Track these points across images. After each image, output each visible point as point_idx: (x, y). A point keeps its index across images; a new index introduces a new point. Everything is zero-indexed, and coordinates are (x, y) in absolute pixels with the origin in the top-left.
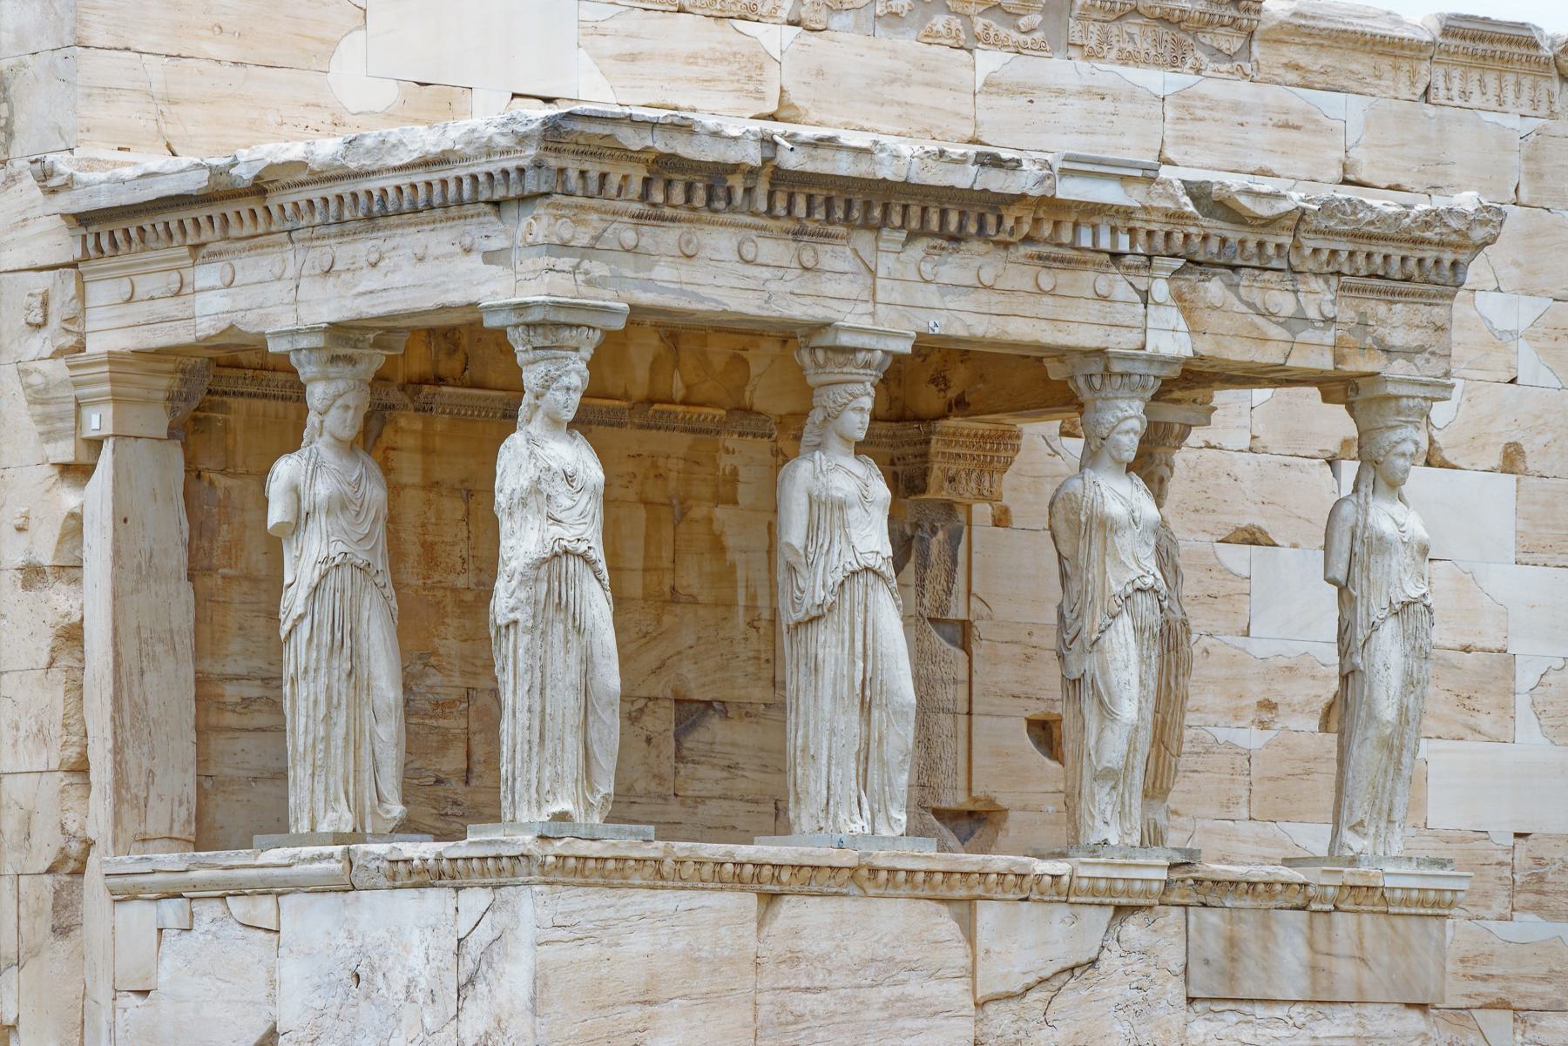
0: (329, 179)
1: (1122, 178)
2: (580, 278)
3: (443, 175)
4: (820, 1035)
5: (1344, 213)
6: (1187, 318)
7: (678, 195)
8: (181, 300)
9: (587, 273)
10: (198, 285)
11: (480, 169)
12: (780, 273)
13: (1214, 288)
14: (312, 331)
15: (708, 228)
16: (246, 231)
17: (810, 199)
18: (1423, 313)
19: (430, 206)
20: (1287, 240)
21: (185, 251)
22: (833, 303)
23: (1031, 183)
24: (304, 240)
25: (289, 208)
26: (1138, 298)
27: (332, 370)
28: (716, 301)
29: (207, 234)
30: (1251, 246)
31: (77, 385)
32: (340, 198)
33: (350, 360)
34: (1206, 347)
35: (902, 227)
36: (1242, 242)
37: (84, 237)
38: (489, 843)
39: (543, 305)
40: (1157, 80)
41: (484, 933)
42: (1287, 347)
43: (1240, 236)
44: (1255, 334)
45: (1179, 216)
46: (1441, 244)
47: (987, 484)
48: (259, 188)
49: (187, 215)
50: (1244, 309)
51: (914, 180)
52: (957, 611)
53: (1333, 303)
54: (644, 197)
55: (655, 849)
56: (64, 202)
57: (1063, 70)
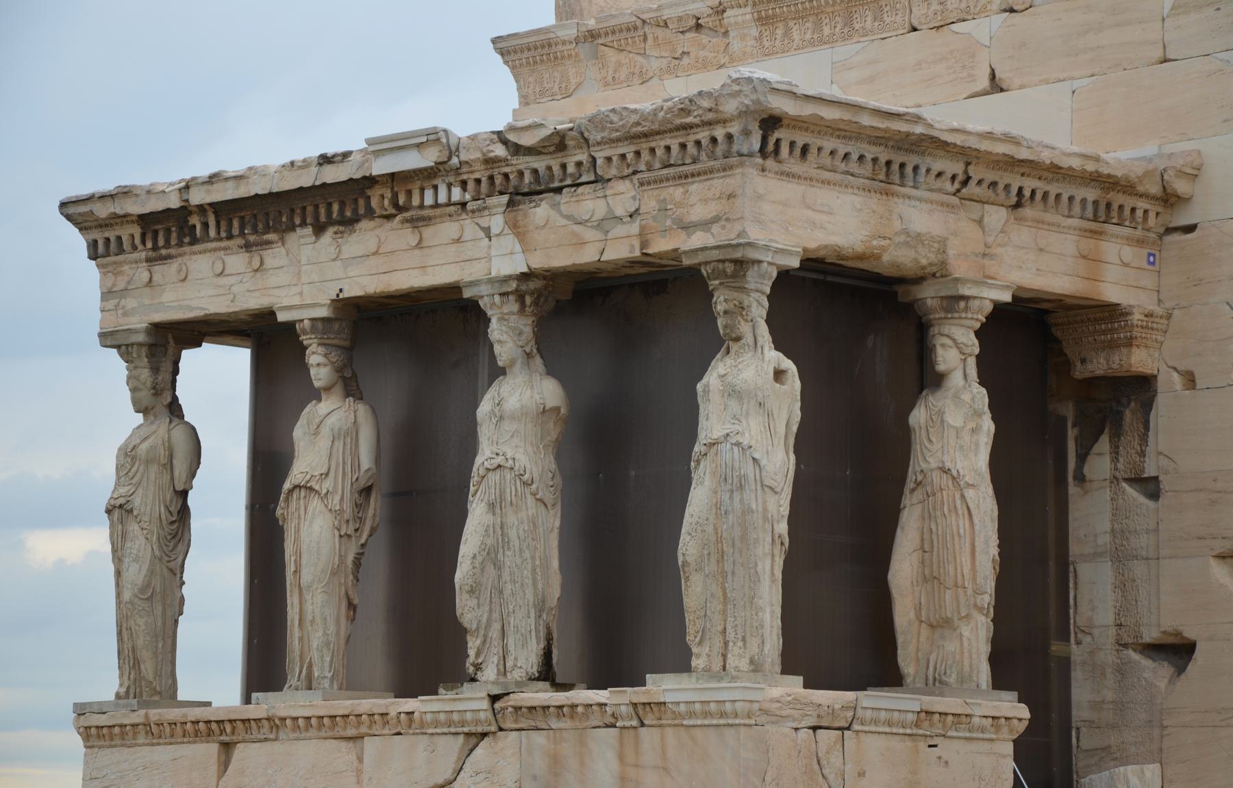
1: (418, 146)
5: (611, 123)
6: (521, 241)
9: (123, 307)
12: (239, 278)
13: (540, 212)
15: (194, 257)
17: (242, 218)
18: (718, 184)
20: (583, 157)
22: (276, 292)
23: (354, 168)
26: (482, 234)
28: (201, 309)
30: (556, 170)
35: (303, 224)
36: (549, 168)
42: (600, 245)
44: (574, 241)
45: (490, 162)
50: (565, 222)
52: (1150, 471)
53: (634, 198)
55: (138, 717)
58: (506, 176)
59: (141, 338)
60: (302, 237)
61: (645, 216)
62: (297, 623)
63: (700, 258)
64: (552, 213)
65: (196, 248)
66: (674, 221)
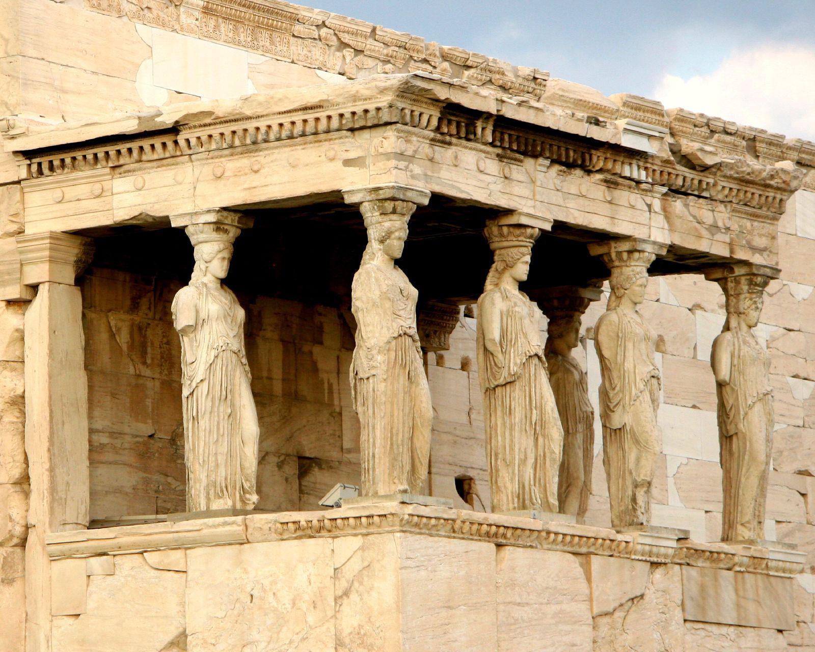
0: (226, 122)
1: (650, 136)
2: (408, 173)
3: (317, 115)
6: (668, 222)
7: (454, 130)
8: (103, 199)
10: (115, 191)
11: (347, 111)
13: (678, 205)
14: (209, 211)
16: (155, 157)
17: (510, 135)
20: (711, 181)
21: (108, 170)
22: (517, 199)
23: (610, 137)
24: (202, 159)
25: (193, 142)
26: (646, 208)
27: (215, 235)
30: (696, 182)
31: (21, 253)
32: (234, 132)
33: (226, 231)
34: (678, 241)
37: (29, 165)
38: (364, 507)
39: (393, 187)
41: (356, 565)
43: (692, 176)
44: (696, 234)
45: (667, 162)
46: (778, 189)
47: (443, 339)
48: (175, 130)
49: (112, 149)
50: (691, 218)
51: (562, 130)
54: (438, 129)
58: (669, 174)
60: (540, 165)
61: (732, 232)
62: (531, 461)
63: (762, 271)
64: (685, 210)
65: (470, 144)
66: (747, 241)
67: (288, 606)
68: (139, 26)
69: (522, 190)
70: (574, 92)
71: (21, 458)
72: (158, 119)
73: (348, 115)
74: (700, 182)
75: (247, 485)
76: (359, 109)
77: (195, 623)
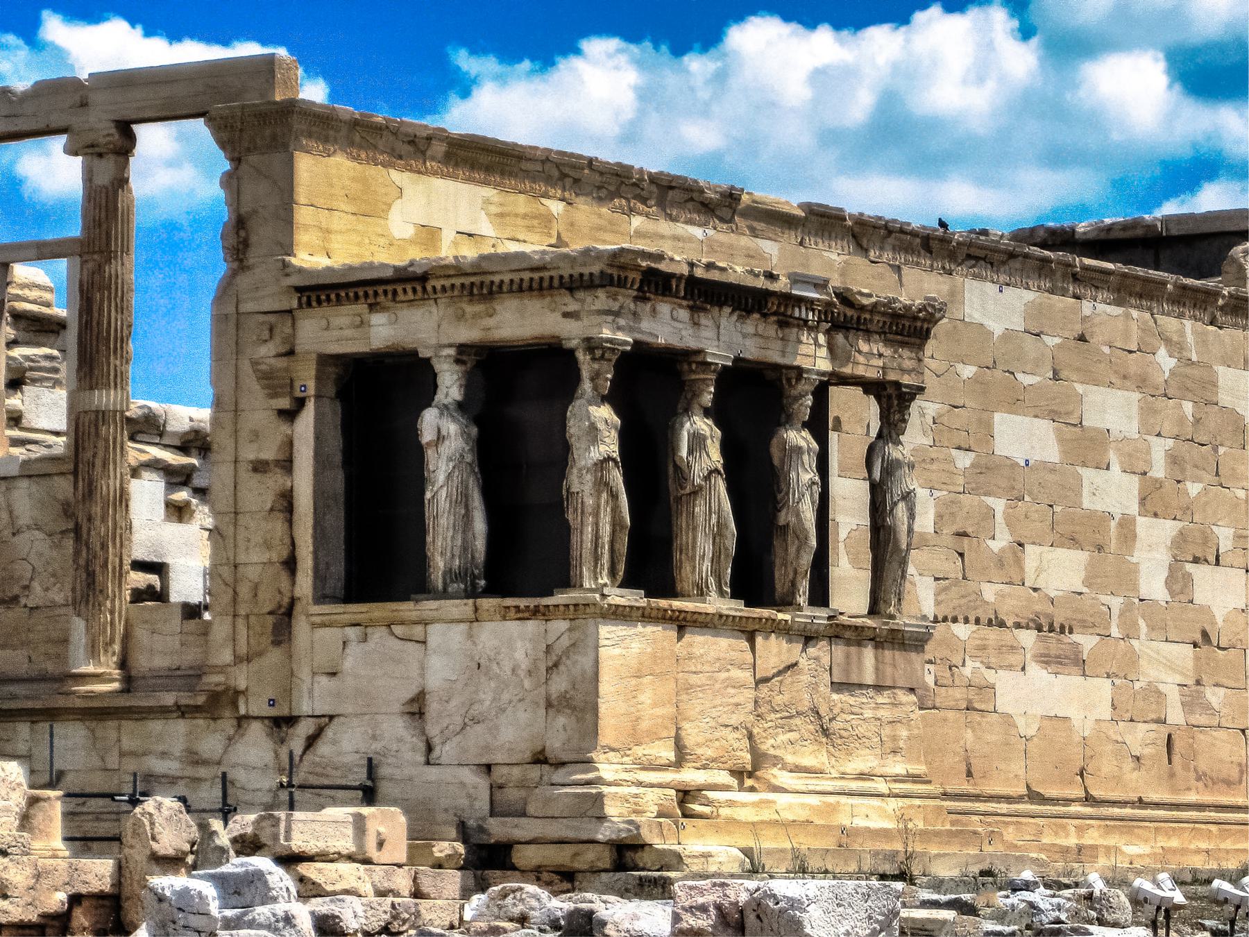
3: (542, 274)
4: (701, 695)
10: (372, 323)
11: (566, 273)
13: (840, 338)
14: (450, 346)
17: (699, 290)
19: (531, 289)
20: (868, 316)
25: (439, 288)
29: (381, 299)
32: (472, 284)
40: (698, 232)
41: (565, 642)
48: (423, 278)
54: (639, 290)
55: (643, 602)
56: (295, 280)
57: (665, 227)
59: (629, 348)
67: (509, 673)
68: (392, 171)
69: (708, 333)
70: (764, 203)
71: (287, 541)
72: (411, 269)
73: (567, 279)
74: (859, 318)
75: (476, 572)
76: (576, 271)
77: (434, 682)
